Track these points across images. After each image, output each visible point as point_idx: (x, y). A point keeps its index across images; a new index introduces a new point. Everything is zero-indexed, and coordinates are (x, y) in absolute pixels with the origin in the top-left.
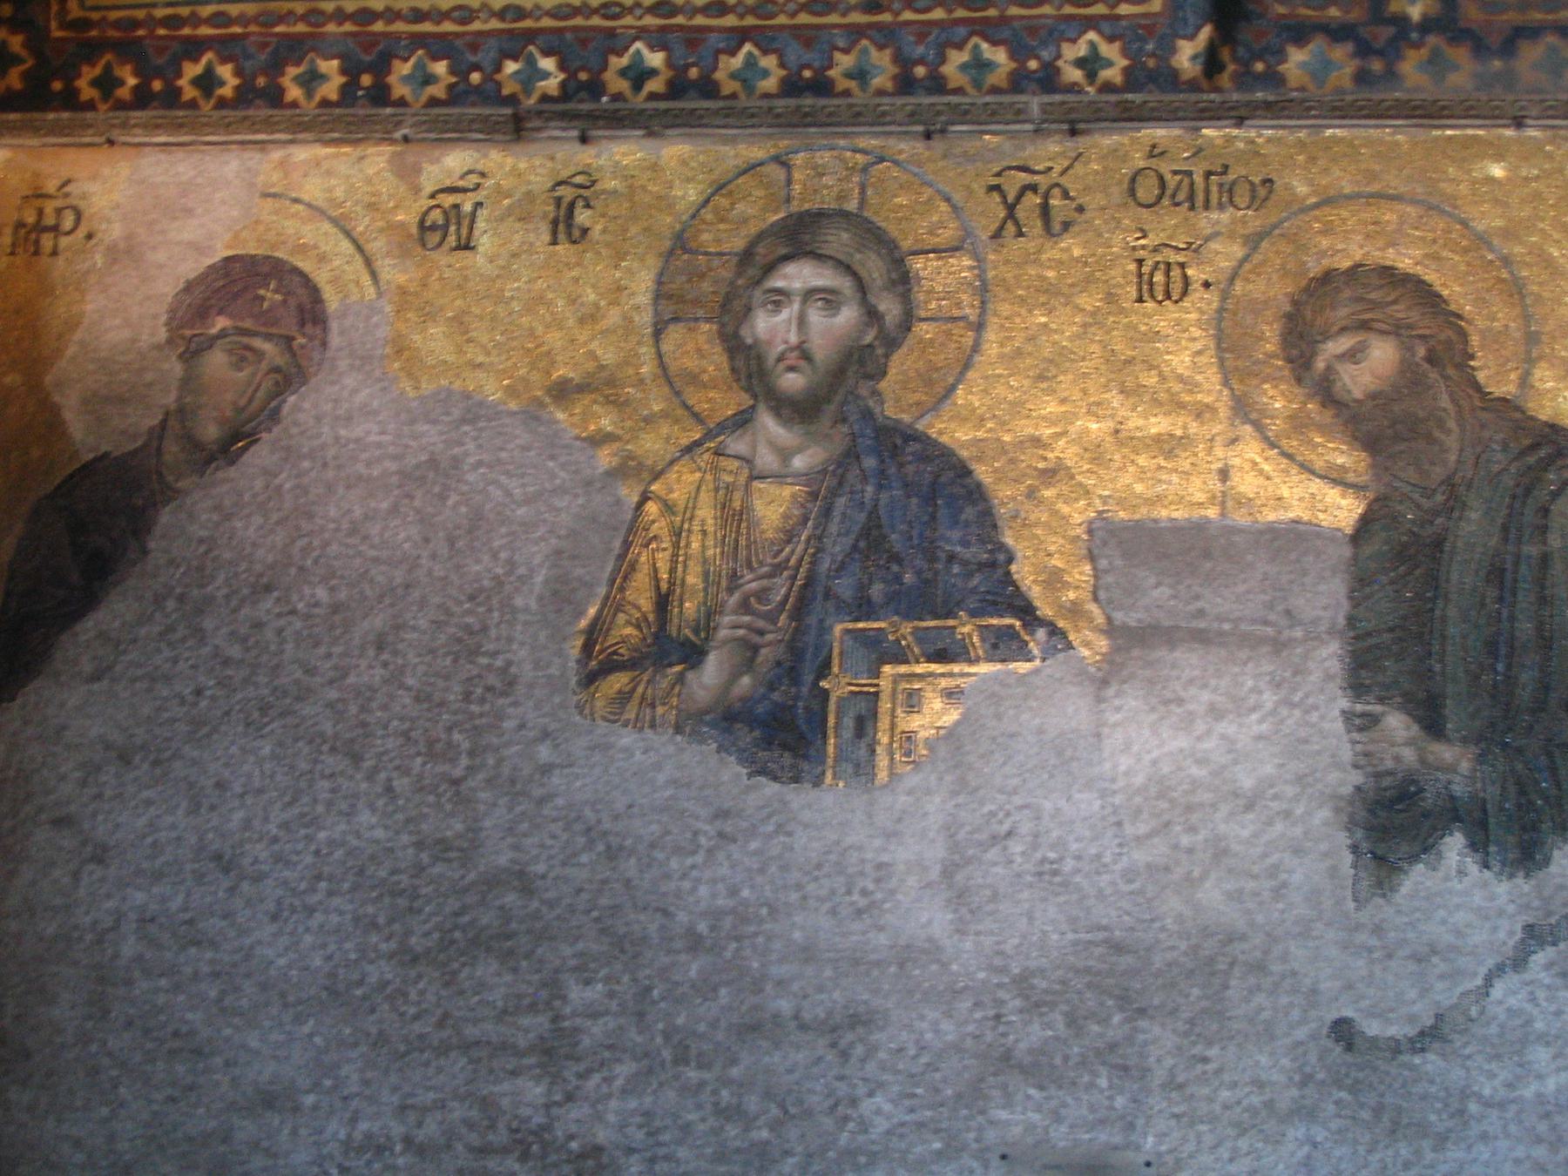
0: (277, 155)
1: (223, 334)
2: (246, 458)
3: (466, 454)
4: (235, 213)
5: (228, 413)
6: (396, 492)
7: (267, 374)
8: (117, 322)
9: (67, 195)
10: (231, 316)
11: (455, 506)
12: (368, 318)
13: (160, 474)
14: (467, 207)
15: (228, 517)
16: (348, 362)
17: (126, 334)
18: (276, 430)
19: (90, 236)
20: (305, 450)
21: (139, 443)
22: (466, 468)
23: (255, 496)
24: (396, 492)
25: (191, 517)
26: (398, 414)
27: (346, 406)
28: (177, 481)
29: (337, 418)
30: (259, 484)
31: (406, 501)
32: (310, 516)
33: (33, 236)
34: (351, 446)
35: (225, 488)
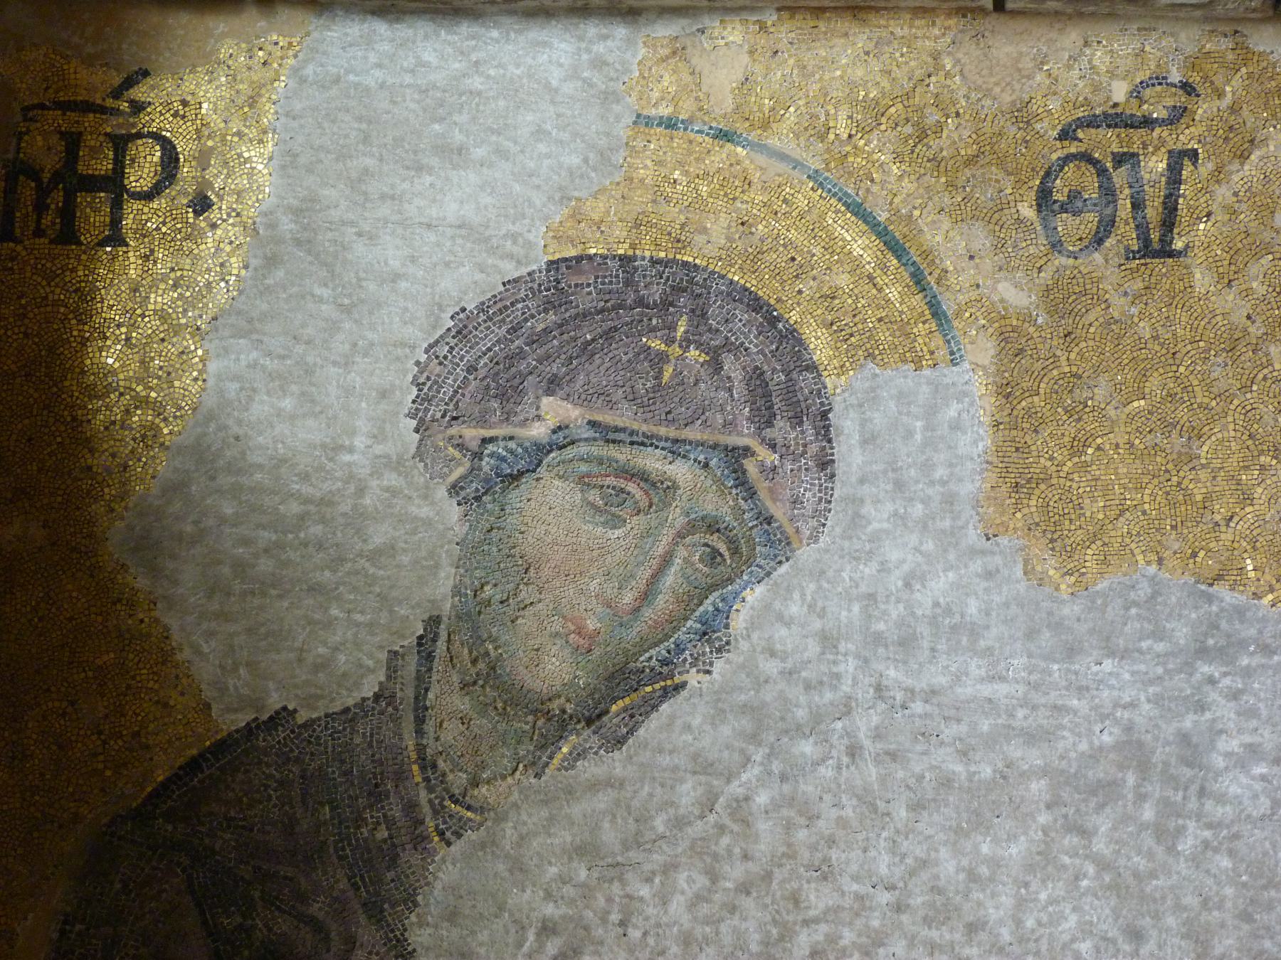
0: (665, 30)
1: (562, 438)
2: (650, 728)
3: (1216, 731)
4: (575, 160)
5: (591, 624)
6: (1043, 818)
7: (680, 535)
8: (287, 404)
9: (138, 107)
10: (584, 400)
11: (1195, 861)
12: (931, 411)
13: (428, 765)
14: (1156, 165)
15: (618, 870)
16: (890, 507)
17: (310, 432)
18: (719, 666)
19: (202, 204)
20: (801, 714)
21: (369, 689)
22: (1220, 762)
23: (680, 823)
24: (1043, 818)
25: (518, 867)
26: (1031, 634)
27: (896, 611)
28: (475, 783)
29: (878, 639)
30: (688, 793)
31: (1071, 840)
32: (824, 872)
33: (57, 198)
34: (918, 707)
35: (602, 801)
